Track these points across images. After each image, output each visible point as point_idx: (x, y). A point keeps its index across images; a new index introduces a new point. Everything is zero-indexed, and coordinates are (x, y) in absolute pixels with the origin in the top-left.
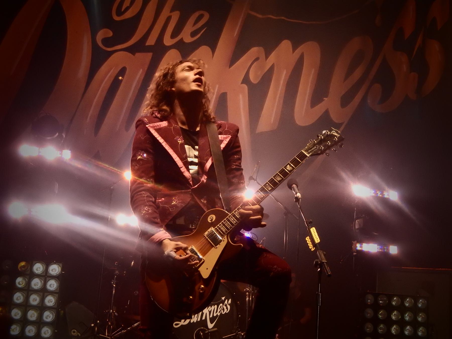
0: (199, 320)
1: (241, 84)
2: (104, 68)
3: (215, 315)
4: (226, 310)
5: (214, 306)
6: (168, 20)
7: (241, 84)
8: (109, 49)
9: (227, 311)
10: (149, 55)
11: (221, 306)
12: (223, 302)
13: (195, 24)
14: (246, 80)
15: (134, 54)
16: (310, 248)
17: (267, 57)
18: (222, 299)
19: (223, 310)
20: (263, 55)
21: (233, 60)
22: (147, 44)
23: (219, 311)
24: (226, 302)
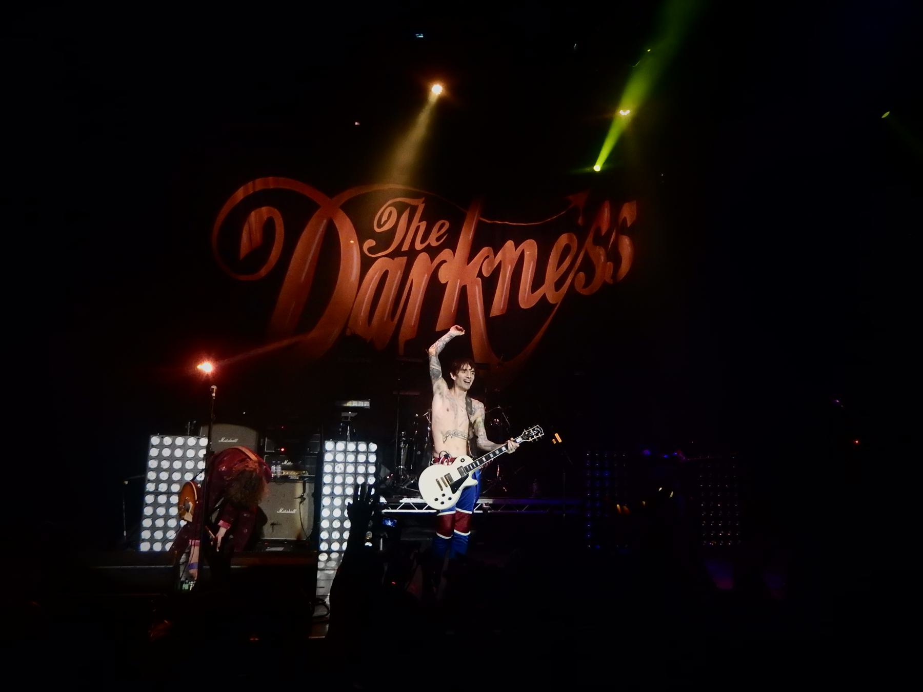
1: (477, 277)
2: (371, 271)
6: (418, 228)
7: (477, 277)
8: (373, 256)
10: (404, 260)
13: (438, 232)
14: (480, 274)
15: (393, 259)
17: (495, 255)
20: (492, 255)
21: (470, 258)
22: (402, 250)
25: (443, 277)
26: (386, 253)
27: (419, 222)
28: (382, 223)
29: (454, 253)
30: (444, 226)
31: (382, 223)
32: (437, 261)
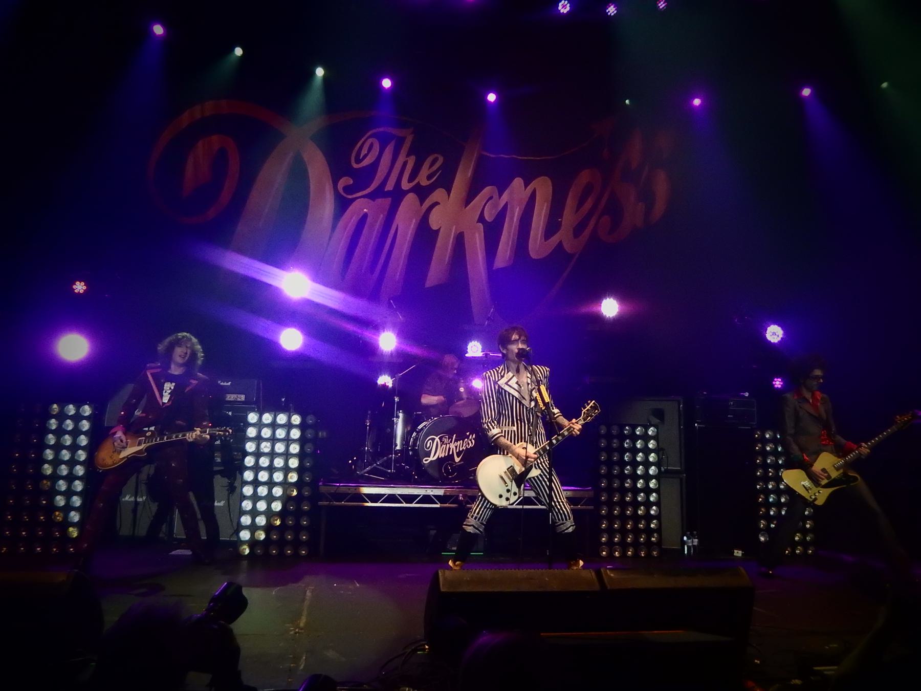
0: (446, 455)
1: (477, 222)
3: (461, 449)
4: (470, 444)
6: (405, 164)
7: (477, 222)
8: (350, 197)
10: (388, 201)
12: (468, 437)
13: (431, 166)
14: (481, 219)
15: (374, 201)
16: (541, 407)
17: (500, 198)
20: (496, 196)
21: (469, 199)
22: (386, 190)
23: (464, 445)
25: (435, 221)
26: (362, 194)
27: (406, 157)
28: (361, 157)
29: (449, 195)
30: (436, 162)
31: (361, 157)
32: (427, 203)
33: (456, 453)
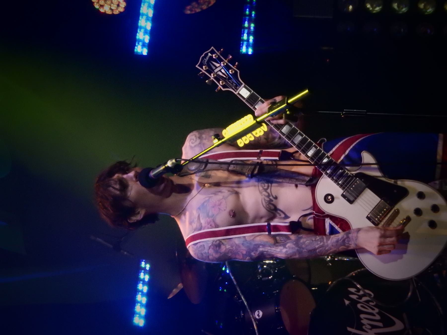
3: (378, 317)
5: (362, 319)
9: (371, 295)
11: (362, 306)
12: (354, 303)
18: (348, 305)
19: (369, 304)
23: (370, 311)
24: (354, 297)
33: (385, 326)
